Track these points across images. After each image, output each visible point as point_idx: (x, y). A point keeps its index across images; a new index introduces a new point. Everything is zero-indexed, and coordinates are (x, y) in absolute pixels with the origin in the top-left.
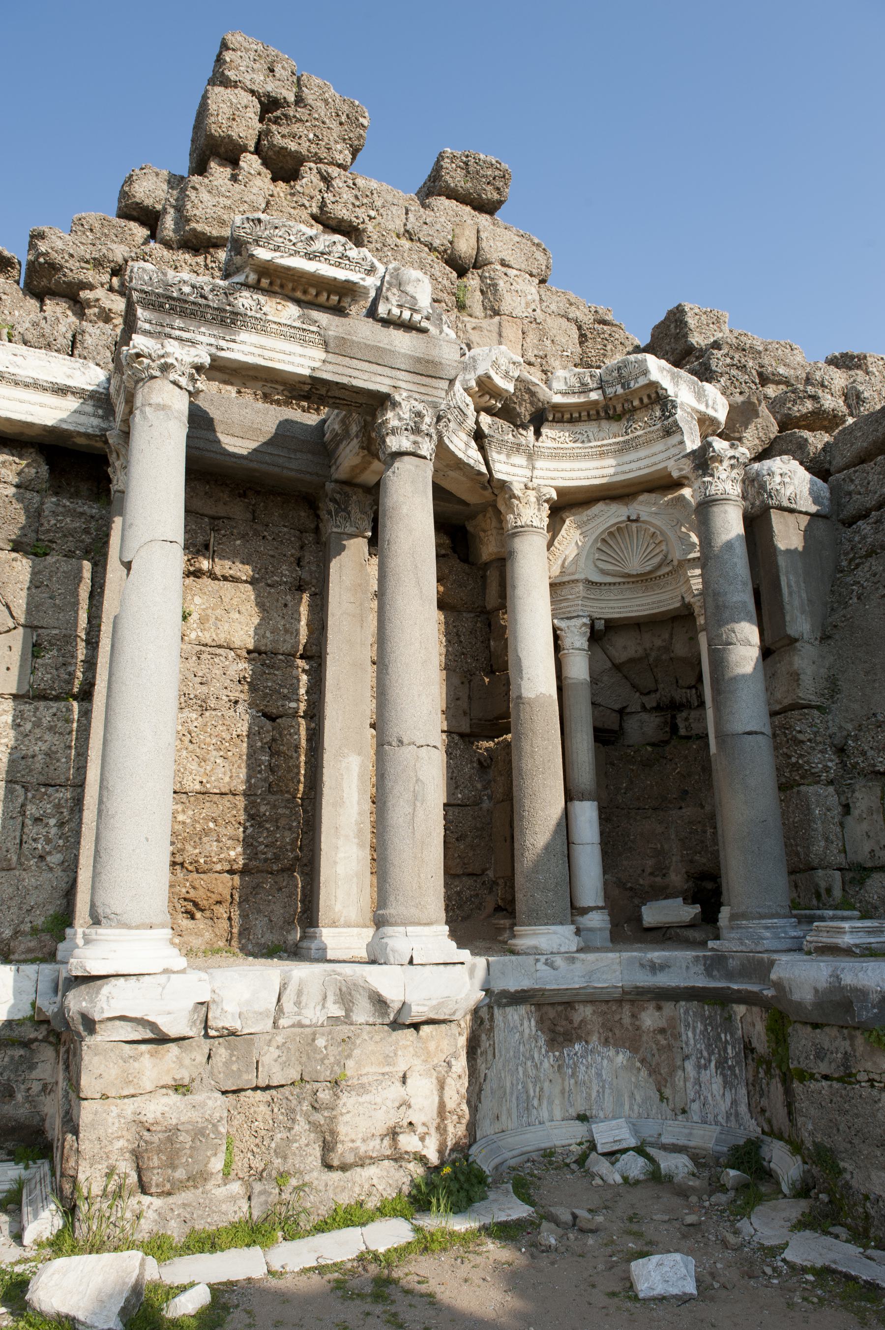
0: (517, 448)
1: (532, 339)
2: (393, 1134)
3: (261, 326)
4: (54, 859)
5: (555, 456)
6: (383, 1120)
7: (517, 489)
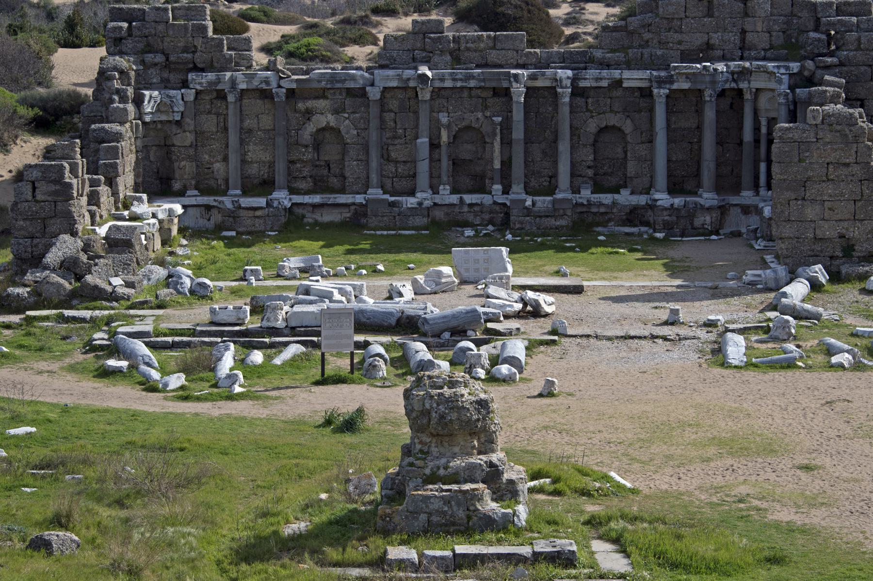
0: (745, 80)
1: (766, 23)
2: (703, 225)
3: (678, 81)
4: (648, 175)
5: (755, 81)
6: (701, 222)
7: (745, 90)
